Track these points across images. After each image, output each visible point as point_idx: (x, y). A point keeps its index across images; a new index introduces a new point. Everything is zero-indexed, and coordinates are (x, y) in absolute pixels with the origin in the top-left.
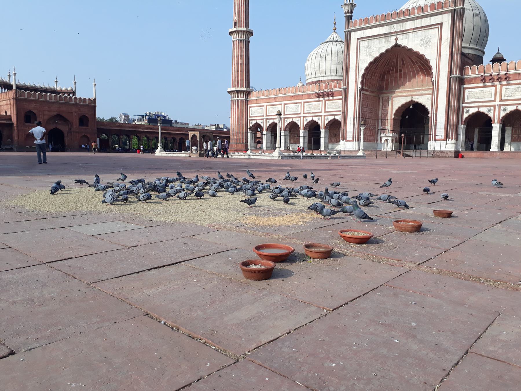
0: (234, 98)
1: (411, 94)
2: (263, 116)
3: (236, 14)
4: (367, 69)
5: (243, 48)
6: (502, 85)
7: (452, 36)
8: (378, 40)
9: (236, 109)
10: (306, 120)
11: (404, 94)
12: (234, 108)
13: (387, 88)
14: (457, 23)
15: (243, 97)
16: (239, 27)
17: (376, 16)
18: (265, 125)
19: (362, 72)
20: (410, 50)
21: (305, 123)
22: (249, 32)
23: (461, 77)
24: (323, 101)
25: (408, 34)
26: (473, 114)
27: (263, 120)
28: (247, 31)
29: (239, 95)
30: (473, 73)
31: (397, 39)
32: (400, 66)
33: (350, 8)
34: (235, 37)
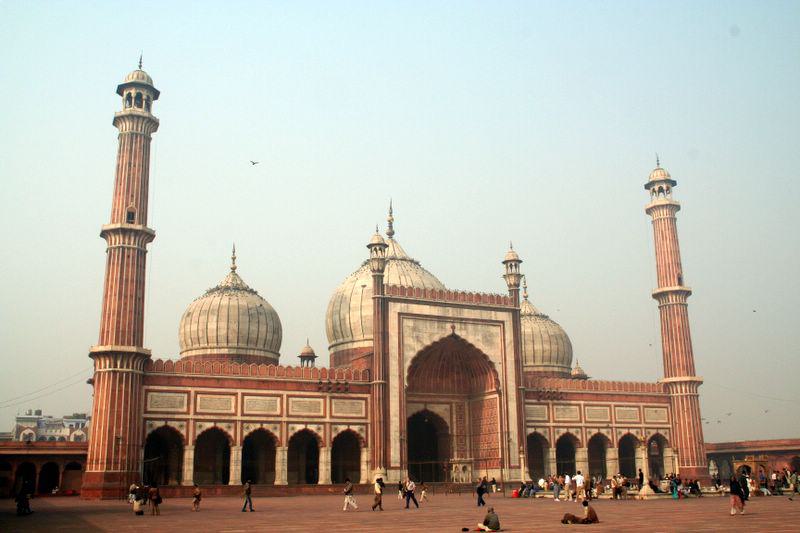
0: (122, 367)
1: (424, 400)
3: (132, 196)
4: (415, 360)
8: (428, 324)
9: (126, 393)
10: (293, 429)
11: (416, 400)
12: (120, 391)
18: (190, 434)
19: (408, 364)
20: (471, 345)
21: (291, 434)
22: (147, 234)
24: (328, 401)
27: (185, 423)
31: (453, 328)
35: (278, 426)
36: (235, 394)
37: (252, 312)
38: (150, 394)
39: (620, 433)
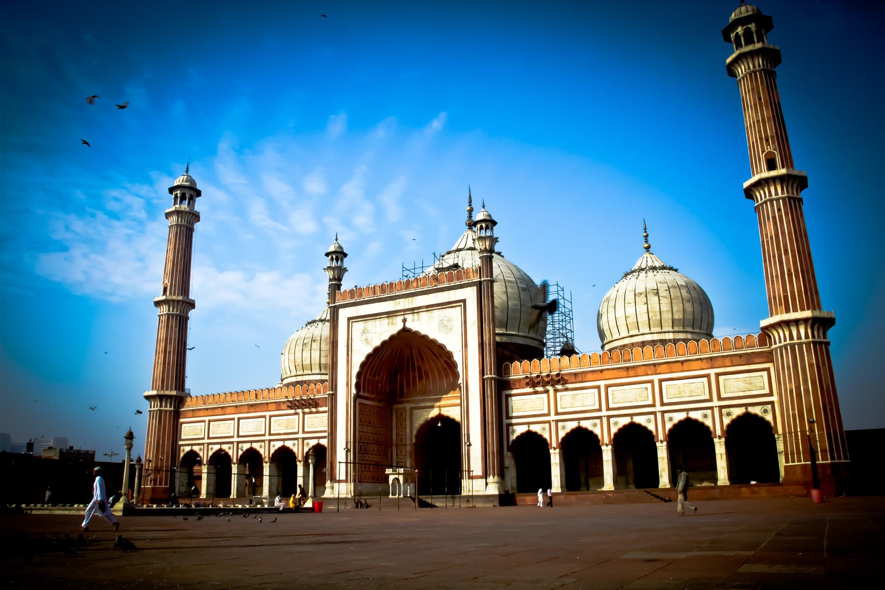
0: (154, 407)
2: (203, 439)
3: (167, 274)
4: (363, 365)
5: (176, 327)
6: (556, 391)
7: (480, 319)
11: (429, 404)
13: (402, 396)
14: (485, 301)
15: (170, 407)
16: (170, 294)
17: (374, 287)
18: (205, 455)
19: (356, 369)
20: (425, 337)
21: (272, 451)
23: (500, 378)
24: (301, 414)
25: (420, 313)
26: (522, 434)
27: (202, 446)
28: (183, 302)
29: (164, 404)
30: (516, 372)
31: (404, 321)
32: (418, 361)
33: (336, 273)
34: (164, 309)
35: (263, 444)
36: (233, 419)
37: (306, 341)
38: (183, 425)
39: (671, 419)
